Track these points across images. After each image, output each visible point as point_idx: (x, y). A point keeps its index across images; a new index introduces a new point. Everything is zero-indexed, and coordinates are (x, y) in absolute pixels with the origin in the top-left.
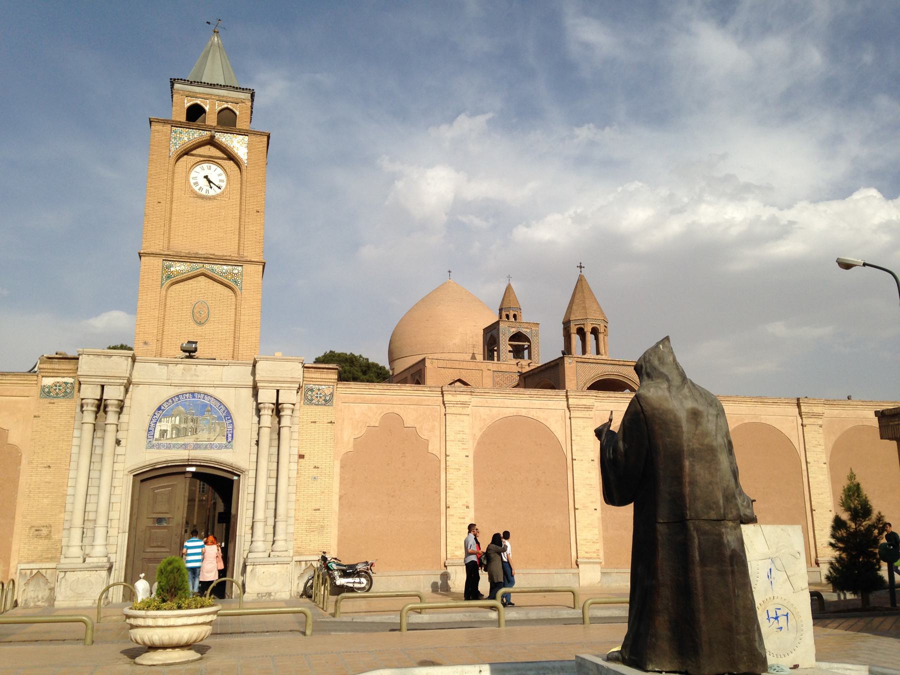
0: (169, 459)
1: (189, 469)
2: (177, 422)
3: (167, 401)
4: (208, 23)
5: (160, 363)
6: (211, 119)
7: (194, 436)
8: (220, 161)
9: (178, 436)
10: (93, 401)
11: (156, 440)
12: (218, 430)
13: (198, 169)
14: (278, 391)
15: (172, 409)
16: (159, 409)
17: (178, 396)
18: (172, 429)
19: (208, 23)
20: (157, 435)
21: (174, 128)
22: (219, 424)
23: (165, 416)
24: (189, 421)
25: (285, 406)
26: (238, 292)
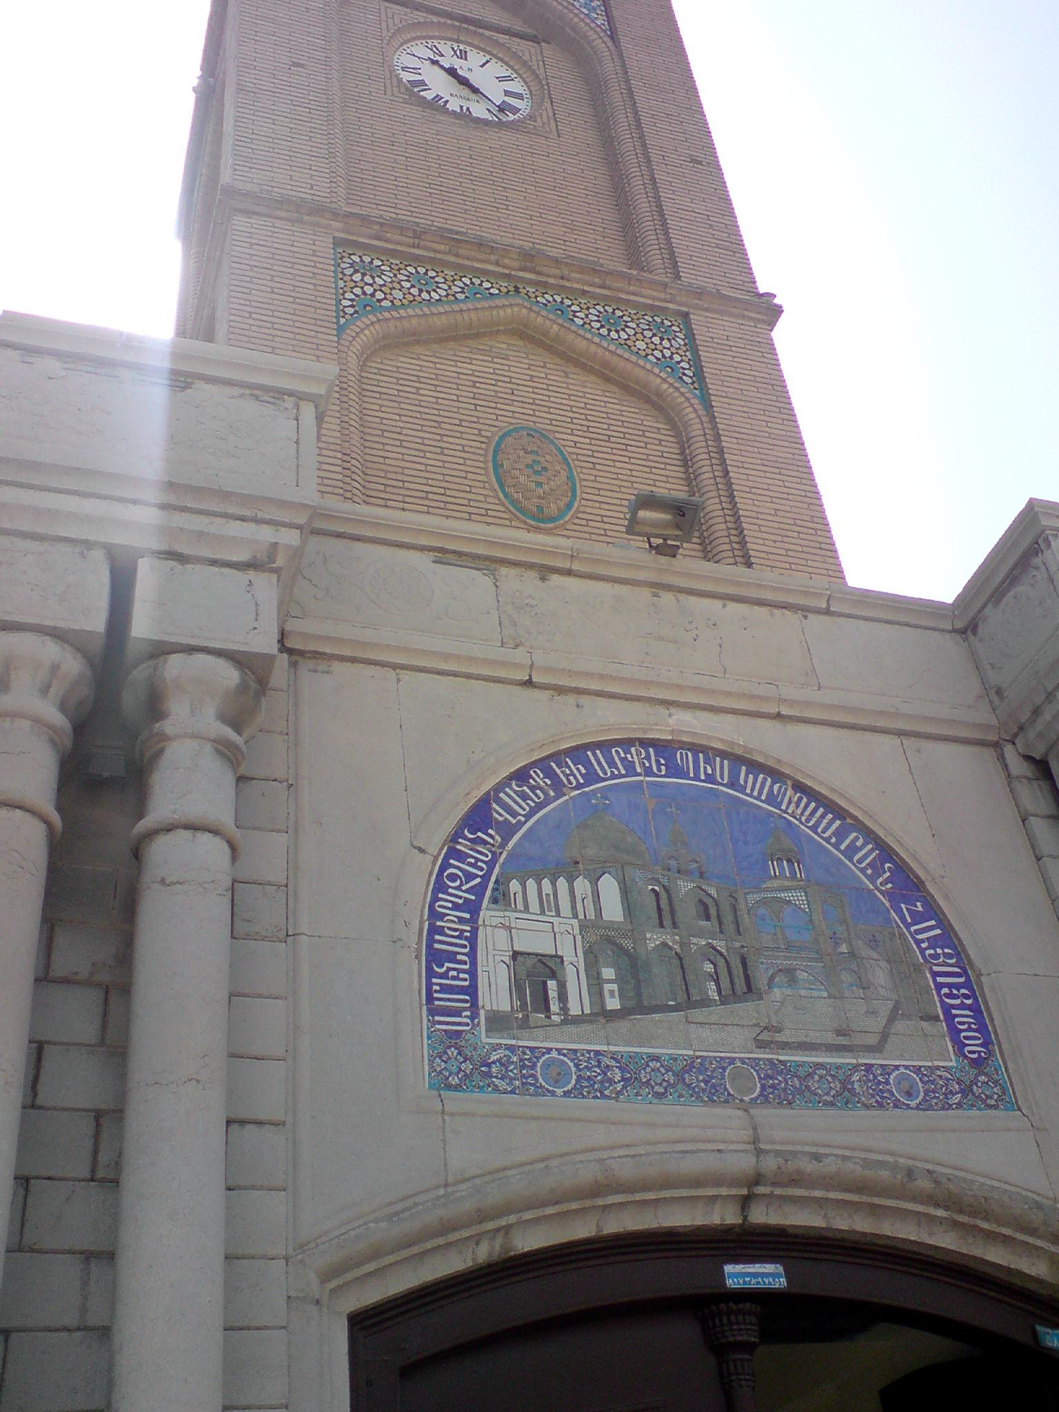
0: (625, 1170)
1: (740, 1275)
2: (613, 910)
3: (521, 776)
5: (443, 555)
7: (747, 1010)
10: (51, 651)
11: (497, 1022)
12: (880, 975)
16: (478, 817)
17: (578, 753)
20: (496, 991)
22: (873, 943)
23: (524, 867)
24: (688, 913)
26: (692, 414)
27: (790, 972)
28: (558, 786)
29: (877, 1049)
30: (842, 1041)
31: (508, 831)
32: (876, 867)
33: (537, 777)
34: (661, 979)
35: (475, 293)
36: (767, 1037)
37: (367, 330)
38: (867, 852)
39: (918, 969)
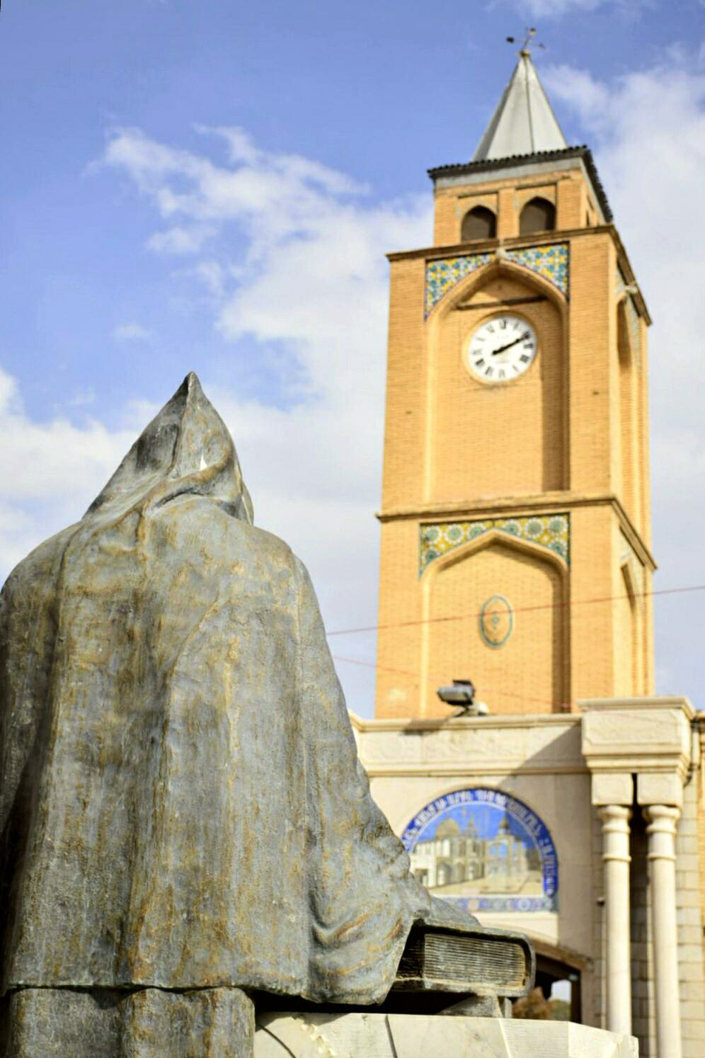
2: (446, 853)
3: (426, 809)
4: (510, 40)
6: (509, 227)
7: (480, 882)
8: (521, 308)
9: (449, 882)
13: (482, 331)
14: (634, 777)
15: (435, 825)
17: (444, 797)
18: (438, 867)
19: (510, 40)
21: (431, 265)
23: (423, 840)
24: (469, 850)
25: (653, 810)
27: (496, 869)
28: (437, 810)
29: (517, 893)
30: (508, 891)
31: (419, 828)
32: (536, 827)
33: (431, 808)
34: (456, 874)
35: (475, 533)
36: (485, 890)
37: (432, 567)
38: (534, 822)
39: (539, 864)
